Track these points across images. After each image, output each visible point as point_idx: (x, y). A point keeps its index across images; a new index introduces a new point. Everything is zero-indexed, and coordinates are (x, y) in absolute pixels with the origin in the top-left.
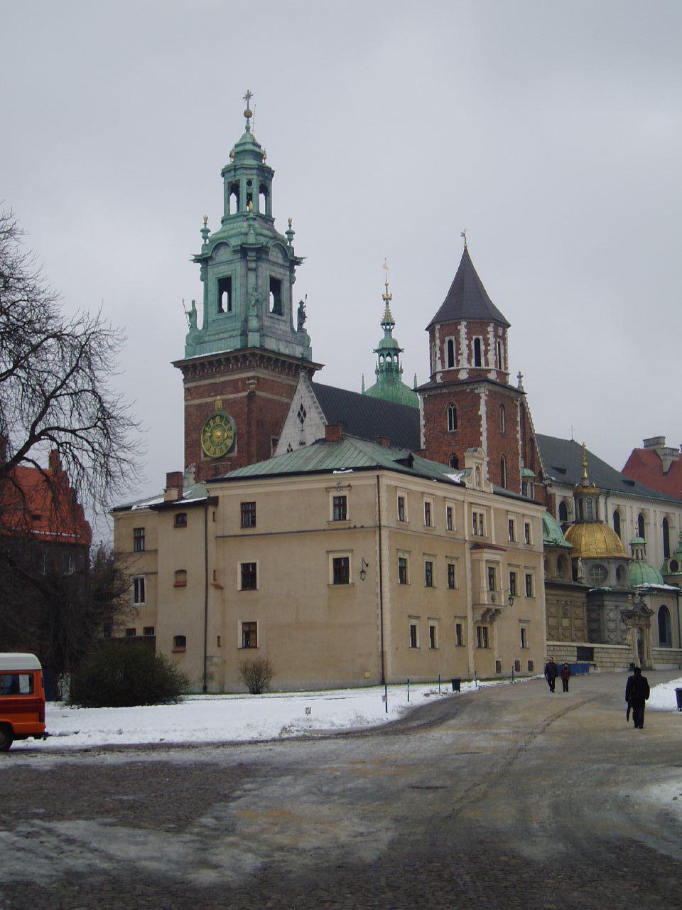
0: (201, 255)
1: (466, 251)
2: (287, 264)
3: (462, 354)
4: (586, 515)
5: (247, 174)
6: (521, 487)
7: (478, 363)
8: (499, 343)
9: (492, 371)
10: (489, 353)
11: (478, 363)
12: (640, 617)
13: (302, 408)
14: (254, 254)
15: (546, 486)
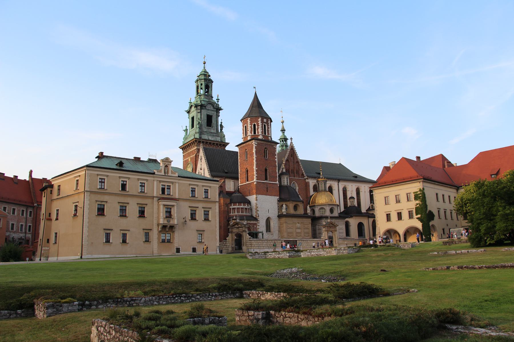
0: (187, 111)
1: (256, 93)
2: (215, 110)
3: (248, 130)
4: (320, 189)
5: (200, 82)
6: (278, 179)
7: (255, 133)
8: (265, 125)
9: (260, 135)
10: (259, 129)
11: (255, 133)
12: (330, 227)
13: (201, 157)
14: (199, 107)
15: (305, 179)
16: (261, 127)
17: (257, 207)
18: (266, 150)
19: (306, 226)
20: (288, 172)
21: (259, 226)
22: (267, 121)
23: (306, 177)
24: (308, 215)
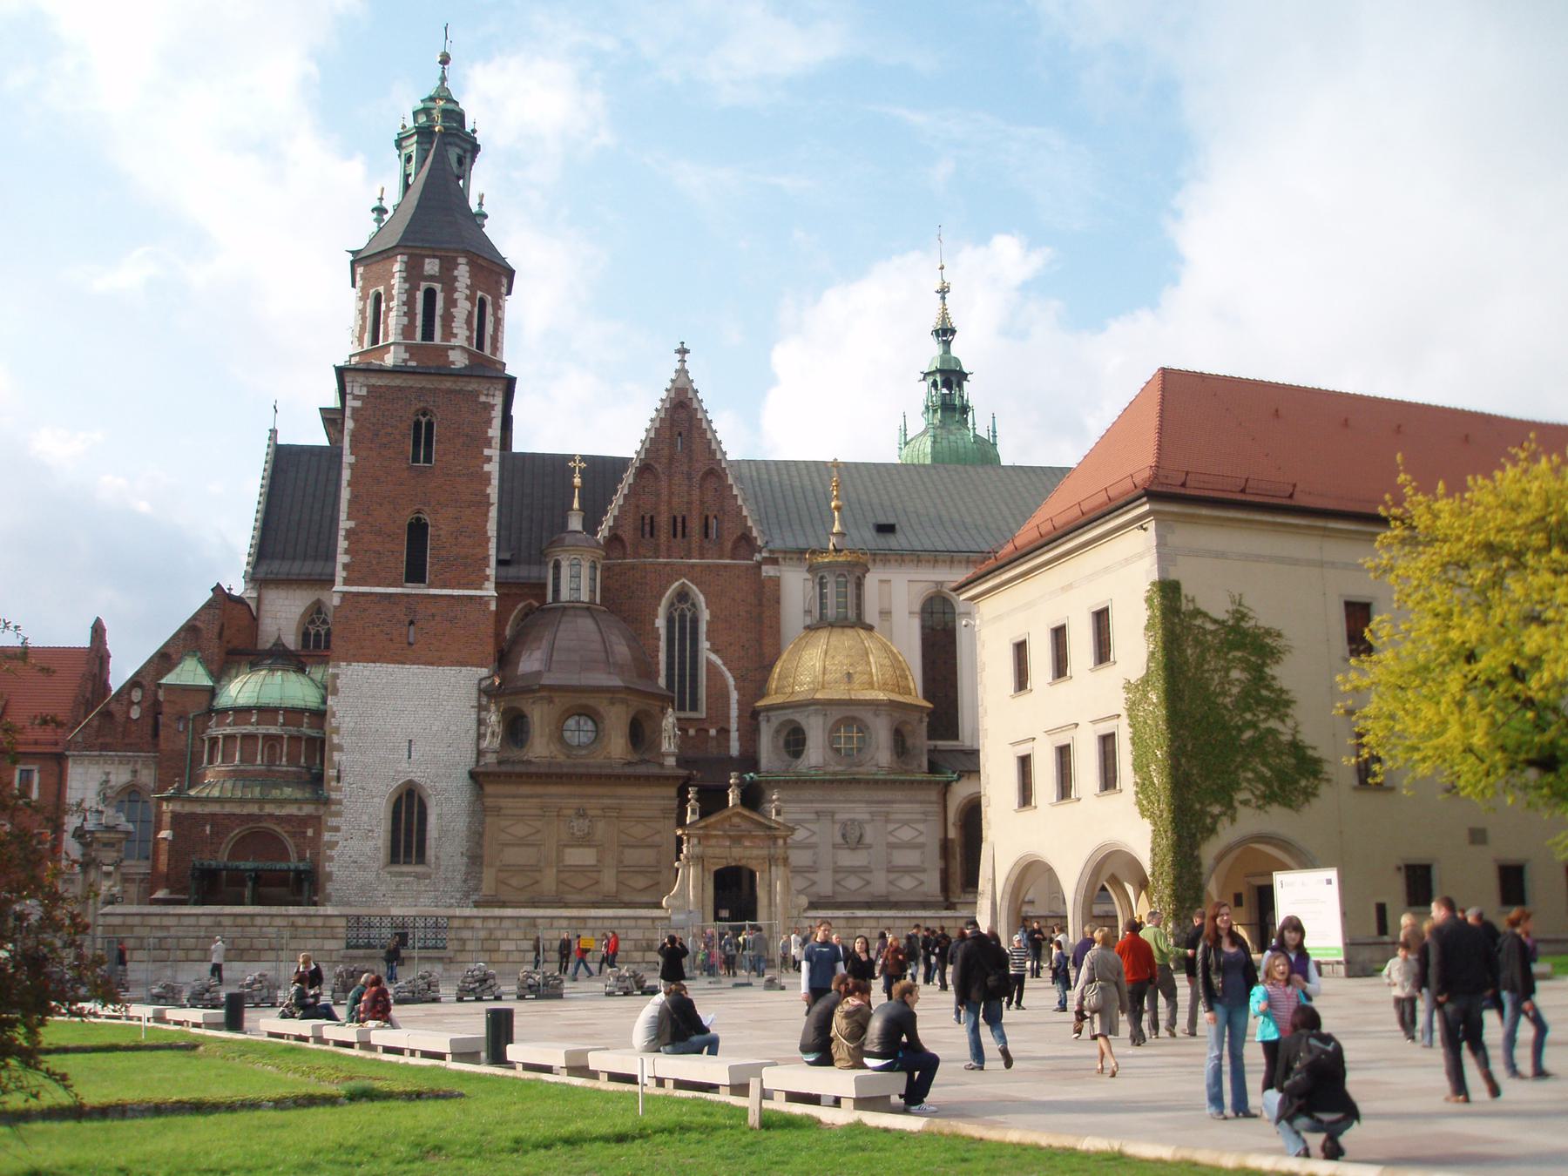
6: (491, 571)
7: (375, 340)
9: (392, 348)
10: (391, 314)
11: (375, 340)
15: (759, 565)
16: (404, 304)
17: (337, 730)
18: (424, 420)
19: (638, 830)
20: (647, 528)
21: (337, 829)
22: (448, 266)
23: (765, 554)
24: (662, 765)
